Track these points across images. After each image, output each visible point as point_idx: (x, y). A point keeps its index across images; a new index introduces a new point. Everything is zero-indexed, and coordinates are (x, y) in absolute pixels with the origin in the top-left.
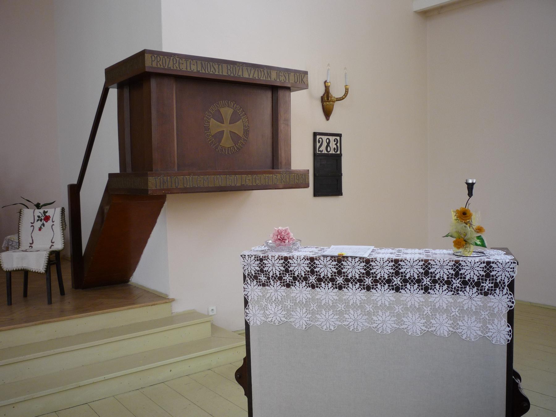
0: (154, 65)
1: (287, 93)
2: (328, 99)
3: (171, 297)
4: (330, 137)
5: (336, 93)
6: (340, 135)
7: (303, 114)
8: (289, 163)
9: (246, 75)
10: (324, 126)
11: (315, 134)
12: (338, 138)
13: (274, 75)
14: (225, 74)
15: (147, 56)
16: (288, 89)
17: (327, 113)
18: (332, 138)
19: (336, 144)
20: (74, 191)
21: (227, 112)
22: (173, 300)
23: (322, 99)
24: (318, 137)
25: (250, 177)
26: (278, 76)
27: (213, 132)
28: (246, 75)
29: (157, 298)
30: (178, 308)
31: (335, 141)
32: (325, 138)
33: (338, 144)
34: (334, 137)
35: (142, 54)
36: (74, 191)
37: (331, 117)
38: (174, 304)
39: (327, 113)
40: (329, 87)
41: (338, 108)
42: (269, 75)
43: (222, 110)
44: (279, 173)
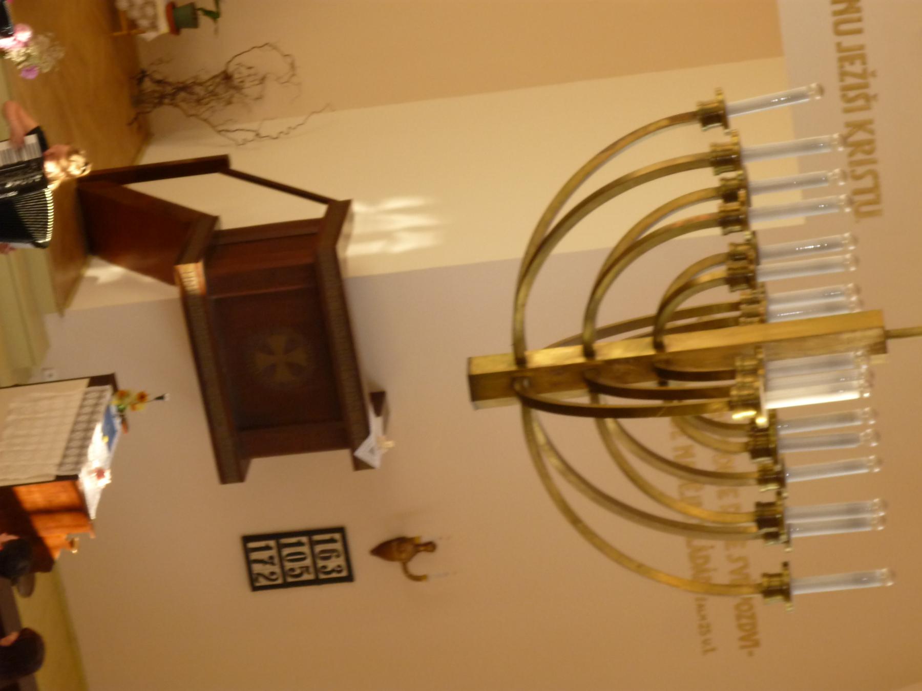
5: (419, 564)
10: (361, 545)
11: (341, 530)
17: (383, 550)
18: (341, 561)
19: (333, 571)
23: (402, 541)
24: (337, 536)
29: (65, 293)
30: (51, 320)
31: (339, 566)
32: (338, 546)
33: (334, 575)
37: (377, 561)
39: (383, 550)
41: (391, 569)
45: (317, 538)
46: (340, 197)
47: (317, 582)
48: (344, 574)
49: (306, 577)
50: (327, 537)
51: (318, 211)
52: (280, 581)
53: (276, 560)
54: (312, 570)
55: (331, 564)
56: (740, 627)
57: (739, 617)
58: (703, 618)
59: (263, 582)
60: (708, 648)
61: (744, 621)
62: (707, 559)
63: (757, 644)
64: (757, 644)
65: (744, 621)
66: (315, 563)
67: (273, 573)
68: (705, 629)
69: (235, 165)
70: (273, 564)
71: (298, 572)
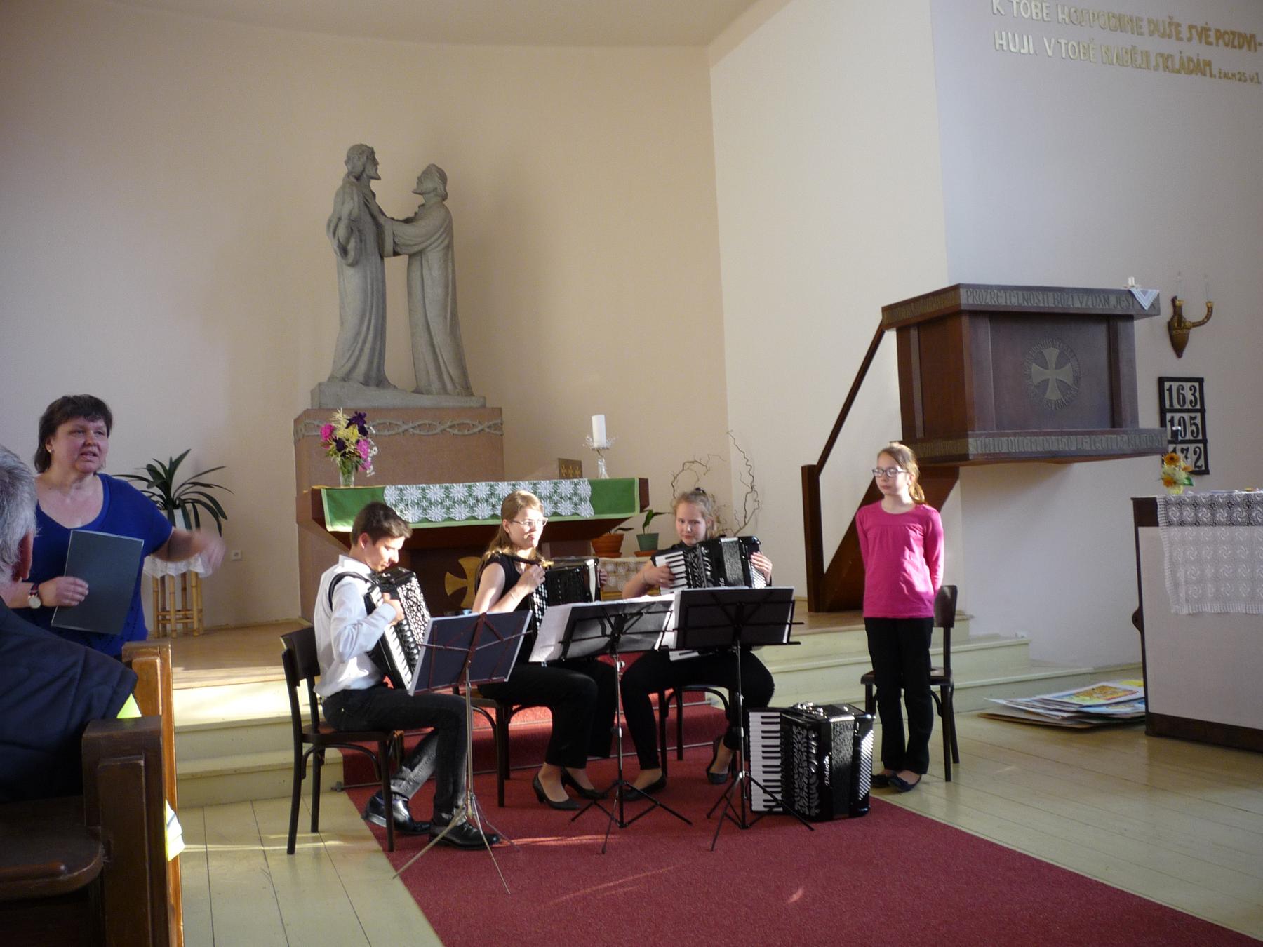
0: (971, 302)
1: (1129, 324)
2: (1179, 325)
3: (969, 612)
4: (1184, 384)
5: (1192, 313)
6: (1200, 381)
7: (1149, 354)
8: (1135, 419)
9: (1077, 305)
11: (1161, 381)
12: (1197, 384)
13: (1113, 300)
14: (1051, 305)
15: (962, 292)
16: (1130, 318)
17: (1179, 346)
18: (1187, 385)
20: (811, 476)
21: (1052, 353)
22: (972, 617)
24: (1167, 385)
25: (1087, 439)
26: (1118, 301)
27: (1036, 380)
28: (1077, 305)
32: (1175, 385)
33: (1197, 394)
34: (1189, 384)
35: (955, 288)
36: (811, 476)
37: (1186, 352)
38: (971, 622)
39: (1179, 346)
40: (1180, 307)
41: (1195, 336)
42: (1107, 301)
43: (1046, 352)
44: (1125, 432)
45: (1168, 406)
46: (877, 318)
47: (1202, 411)
48: (1197, 384)
49: (1198, 421)
50: (1167, 393)
51: (891, 338)
52: (1201, 446)
53: (1185, 446)
54: (1193, 415)
55: (1189, 397)
56: (1241, 47)
57: (1234, 47)
58: (1234, 75)
59: (1201, 463)
60: (1255, 79)
61: (1236, 43)
62: (1190, 60)
63: (1253, 36)
64: (1253, 36)
65: (1236, 43)
66: (1188, 411)
67: (1195, 452)
68: (1242, 78)
69: (815, 462)
70: (1187, 450)
71: (1194, 428)
